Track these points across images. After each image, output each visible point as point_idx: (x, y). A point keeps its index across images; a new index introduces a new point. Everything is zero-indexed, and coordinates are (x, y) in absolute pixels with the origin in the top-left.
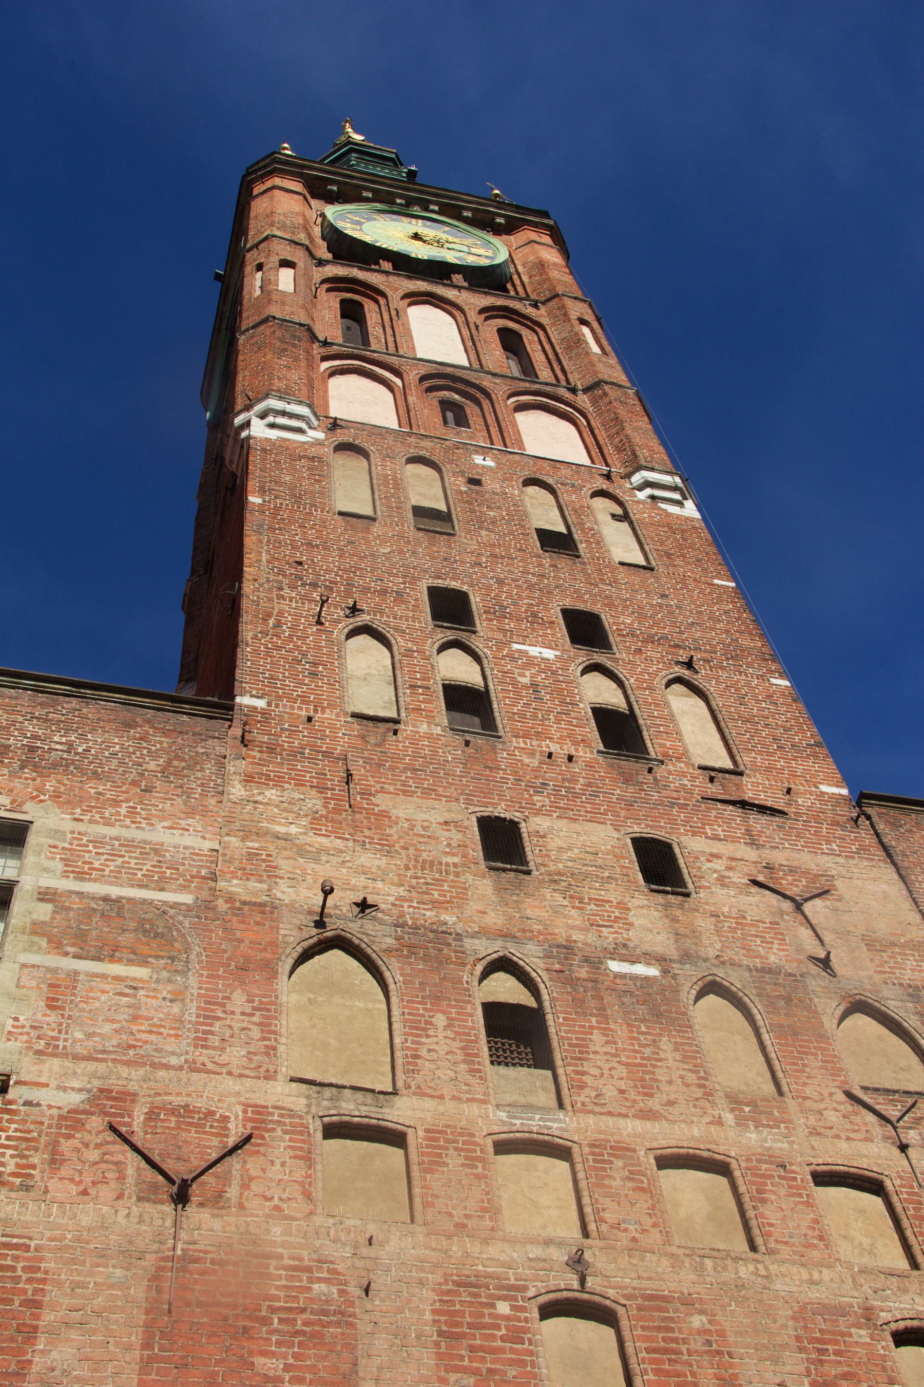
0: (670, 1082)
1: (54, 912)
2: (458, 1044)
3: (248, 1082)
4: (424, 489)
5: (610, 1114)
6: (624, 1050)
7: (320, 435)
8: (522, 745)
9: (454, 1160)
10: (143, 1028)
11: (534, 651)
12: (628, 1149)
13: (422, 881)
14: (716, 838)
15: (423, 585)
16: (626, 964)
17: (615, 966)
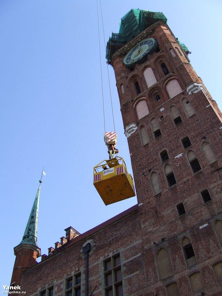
0: (212, 248)
1: (126, 267)
2: (180, 260)
3: (155, 284)
4: (155, 126)
5: (204, 261)
6: (204, 245)
7: (136, 128)
8: (180, 183)
9: (183, 283)
10: (140, 282)
11: (178, 156)
12: (207, 267)
13: (170, 227)
14: (215, 182)
15: (159, 154)
16: (202, 226)
17: (201, 227)
